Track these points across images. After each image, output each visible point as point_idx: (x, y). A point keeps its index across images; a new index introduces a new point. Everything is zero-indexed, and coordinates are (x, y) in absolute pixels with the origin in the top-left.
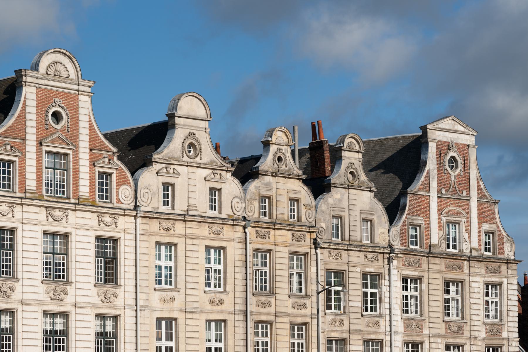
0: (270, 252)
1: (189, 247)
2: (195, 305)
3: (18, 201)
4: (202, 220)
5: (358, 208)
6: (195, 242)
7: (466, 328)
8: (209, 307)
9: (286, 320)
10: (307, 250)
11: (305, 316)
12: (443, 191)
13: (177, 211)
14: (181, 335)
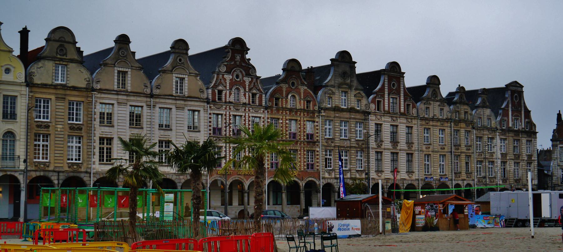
0: (459, 130)
1: (434, 129)
2: (436, 150)
3: (383, 114)
4: (438, 120)
5: (486, 114)
6: (436, 127)
7: (521, 156)
8: (440, 150)
9: (464, 154)
10: (470, 130)
11: (470, 153)
12: (513, 108)
13: (430, 117)
14: (432, 160)
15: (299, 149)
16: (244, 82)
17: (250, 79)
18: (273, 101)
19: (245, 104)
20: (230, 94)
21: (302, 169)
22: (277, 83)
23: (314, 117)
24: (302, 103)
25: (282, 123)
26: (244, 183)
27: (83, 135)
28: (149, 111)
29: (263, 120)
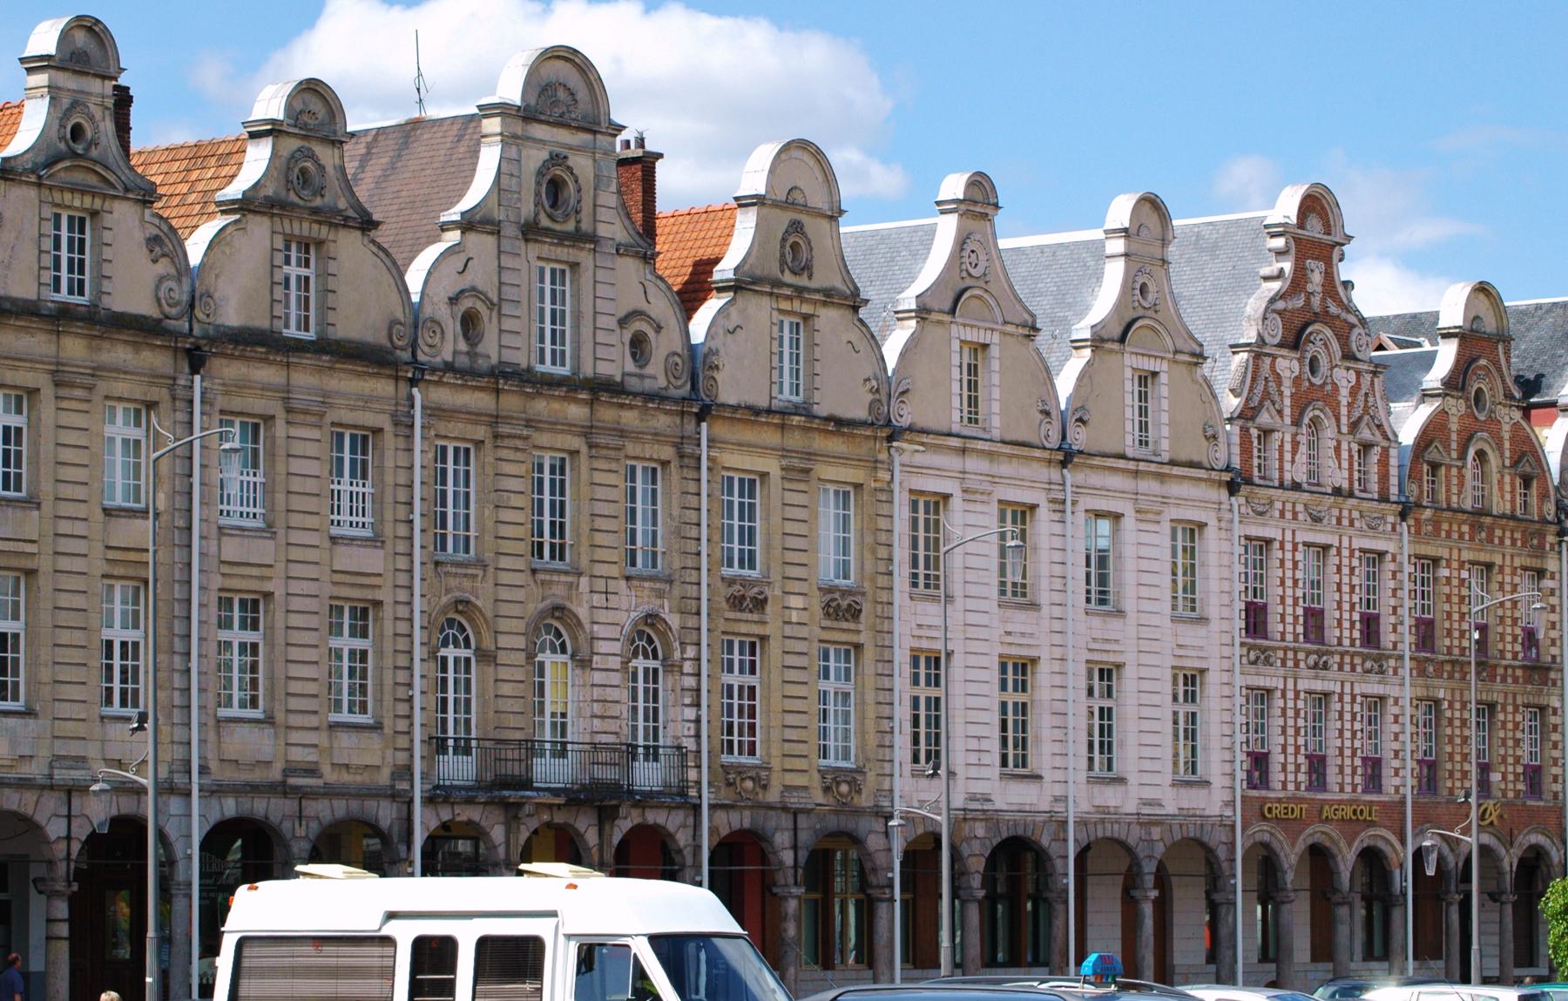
15: (1501, 700)
16: (1336, 388)
17: (1352, 376)
18: (1421, 480)
19: (1337, 492)
20: (1295, 445)
21: (1511, 794)
22: (1426, 396)
23: (1539, 551)
24: (1508, 488)
25: (1448, 579)
26: (1340, 857)
27: (861, 639)
28: (1057, 528)
29: (1392, 566)
